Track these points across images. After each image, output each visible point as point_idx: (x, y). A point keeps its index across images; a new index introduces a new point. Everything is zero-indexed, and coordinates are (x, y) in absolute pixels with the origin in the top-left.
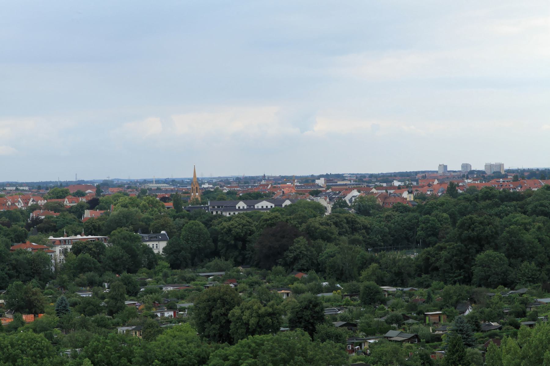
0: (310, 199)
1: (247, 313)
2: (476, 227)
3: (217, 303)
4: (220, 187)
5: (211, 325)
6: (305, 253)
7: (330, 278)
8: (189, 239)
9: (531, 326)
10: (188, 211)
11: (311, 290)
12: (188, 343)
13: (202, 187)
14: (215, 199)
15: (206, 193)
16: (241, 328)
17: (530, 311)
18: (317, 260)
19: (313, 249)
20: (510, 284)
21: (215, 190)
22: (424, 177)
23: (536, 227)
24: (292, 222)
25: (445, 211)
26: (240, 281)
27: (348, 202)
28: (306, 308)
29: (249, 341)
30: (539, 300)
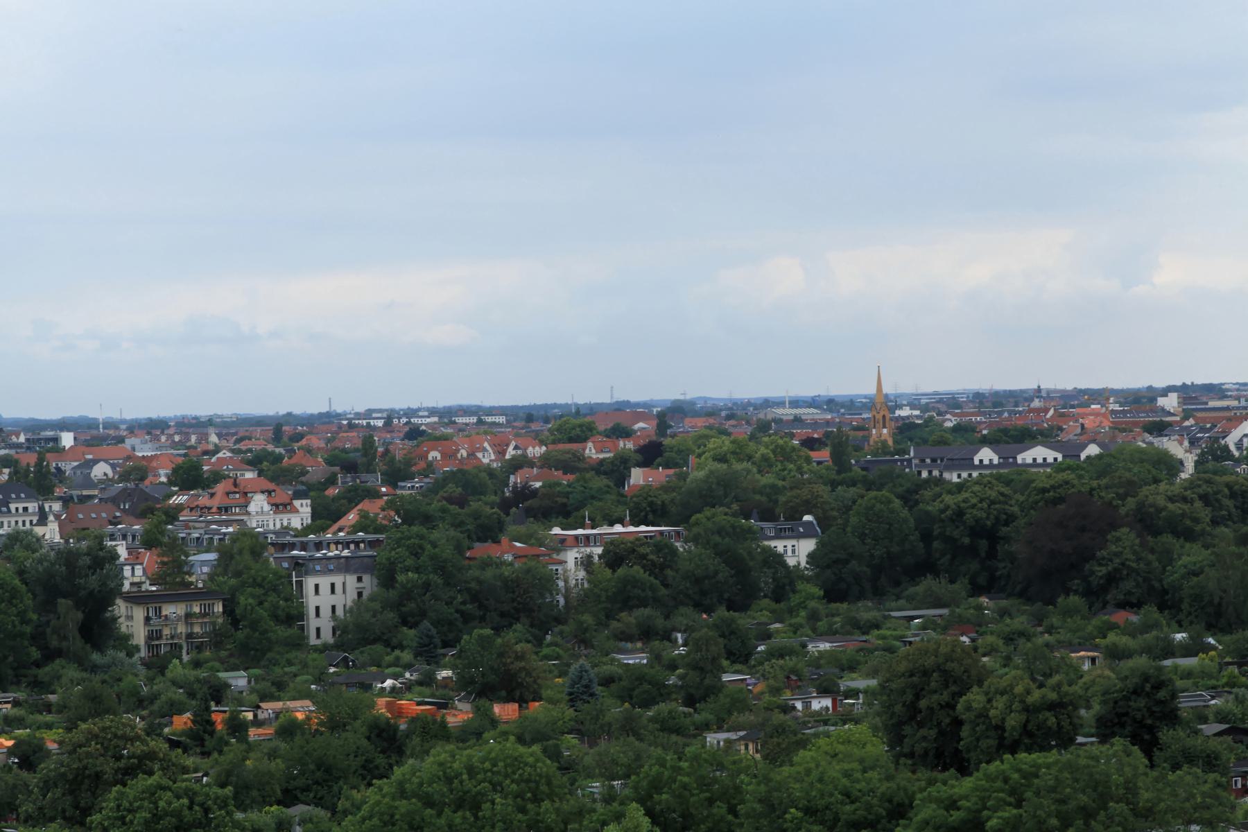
0: (1144, 441)
1: (1000, 703)
3: (931, 679)
4: (937, 415)
5: (918, 730)
6: (1134, 565)
7: (1191, 623)
8: (866, 535)
10: (863, 469)
11: (1147, 650)
12: (864, 771)
13: (896, 415)
14: (925, 441)
15: (906, 429)
16: (988, 737)
18: (1161, 581)
19: (1151, 557)
21: (925, 421)
24: (1103, 494)
26: (983, 629)
27: (1232, 448)
28: (1136, 692)
29: (1005, 767)
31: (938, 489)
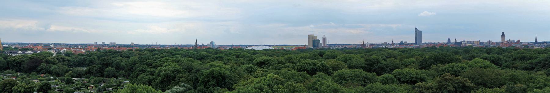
1: (20, 88)
9: (122, 89)
11: (47, 80)
14: (9, 50)
15: (5, 48)
17: (122, 84)
18: (49, 70)
19: (48, 67)
20: (116, 77)
25: (96, 56)
27: (62, 52)
28: (44, 85)
30: (125, 81)
31: (10, 57)
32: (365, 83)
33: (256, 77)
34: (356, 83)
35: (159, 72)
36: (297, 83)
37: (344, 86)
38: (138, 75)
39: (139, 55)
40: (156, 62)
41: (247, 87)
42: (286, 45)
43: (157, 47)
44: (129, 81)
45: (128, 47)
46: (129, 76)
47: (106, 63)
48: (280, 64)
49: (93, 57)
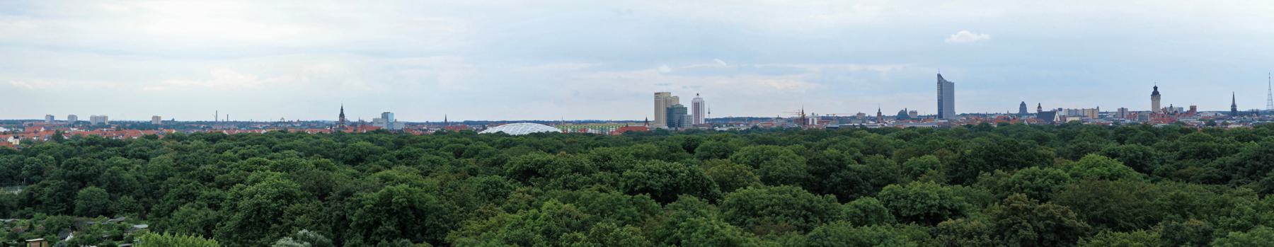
2: (80, 167)
17: (126, 235)
20: (110, 214)
22: (31, 125)
23: (135, 168)
25: (50, 154)
30: (135, 226)
32: (807, 222)
33: (510, 211)
34: (782, 224)
35: (234, 200)
36: (624, 225)
37: (752, 231)
38: (174, 208)
39: (176, 152)
40: (225, 170)
41: (485, 238)
42: (593, 122)
43: (229, 129)
44: (147, 226)
45: (143, 129)
46: (148, 209)
47: (81, 174)
48: (577, 174)
49: (42, 158)
